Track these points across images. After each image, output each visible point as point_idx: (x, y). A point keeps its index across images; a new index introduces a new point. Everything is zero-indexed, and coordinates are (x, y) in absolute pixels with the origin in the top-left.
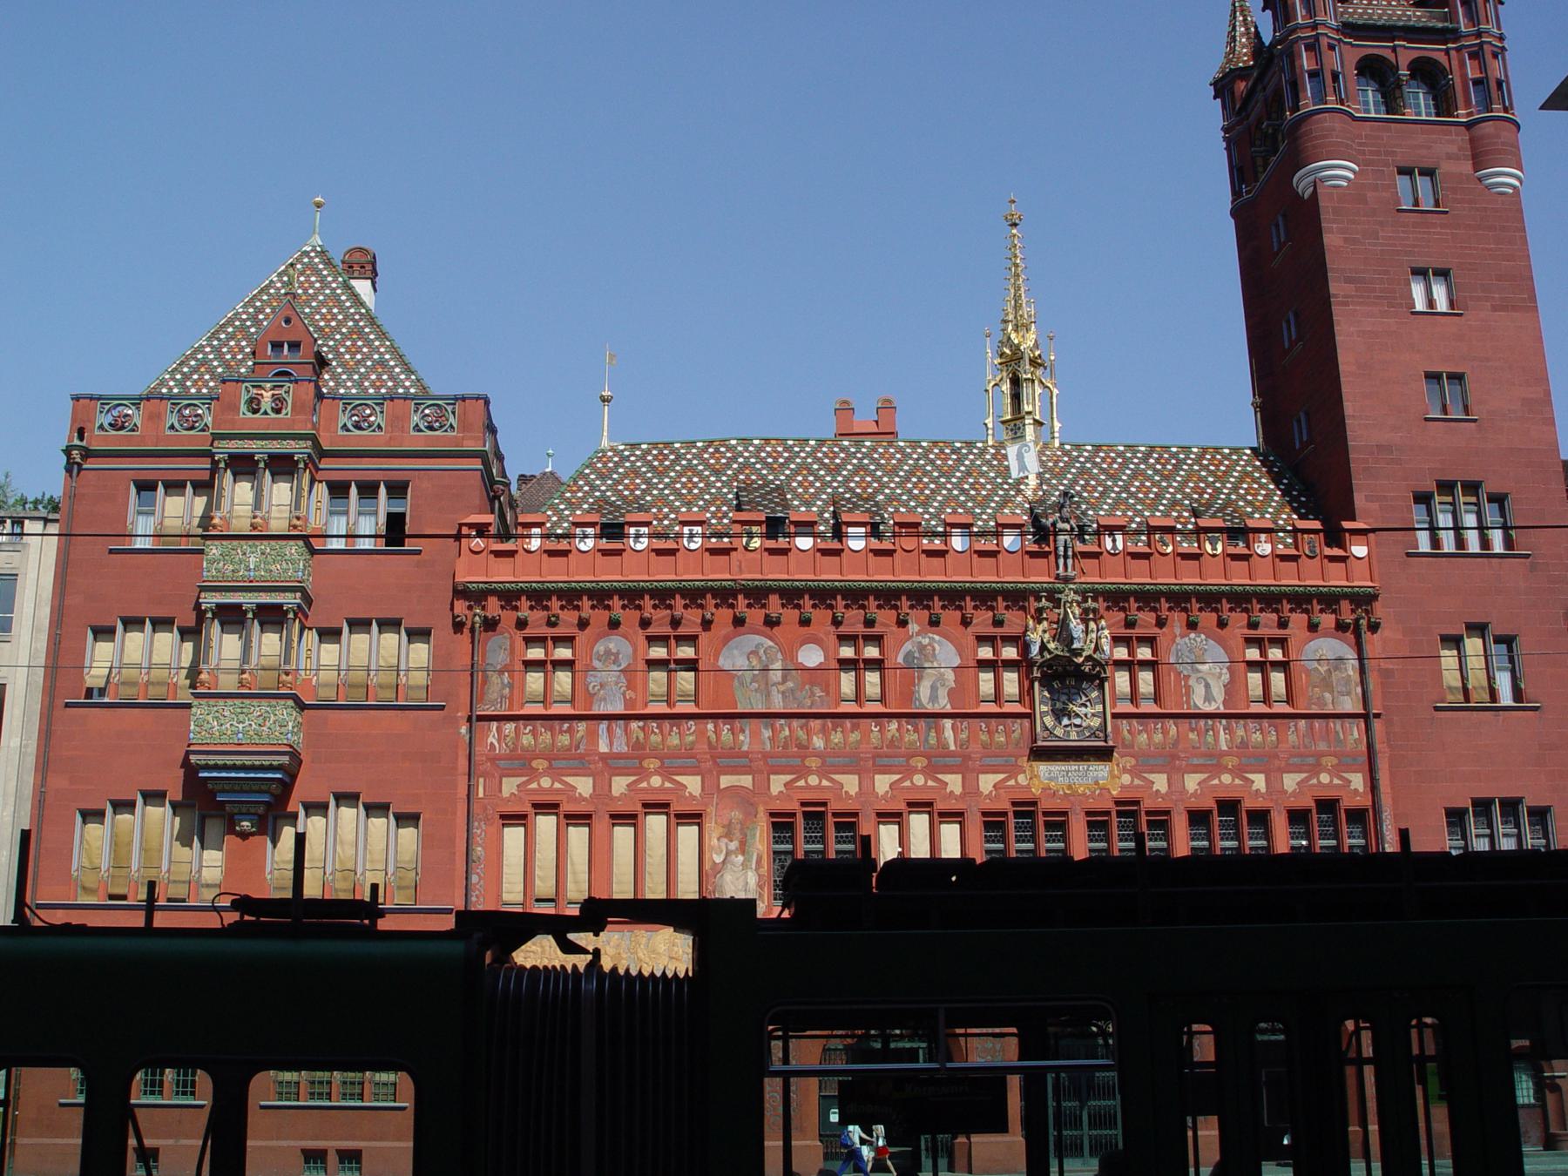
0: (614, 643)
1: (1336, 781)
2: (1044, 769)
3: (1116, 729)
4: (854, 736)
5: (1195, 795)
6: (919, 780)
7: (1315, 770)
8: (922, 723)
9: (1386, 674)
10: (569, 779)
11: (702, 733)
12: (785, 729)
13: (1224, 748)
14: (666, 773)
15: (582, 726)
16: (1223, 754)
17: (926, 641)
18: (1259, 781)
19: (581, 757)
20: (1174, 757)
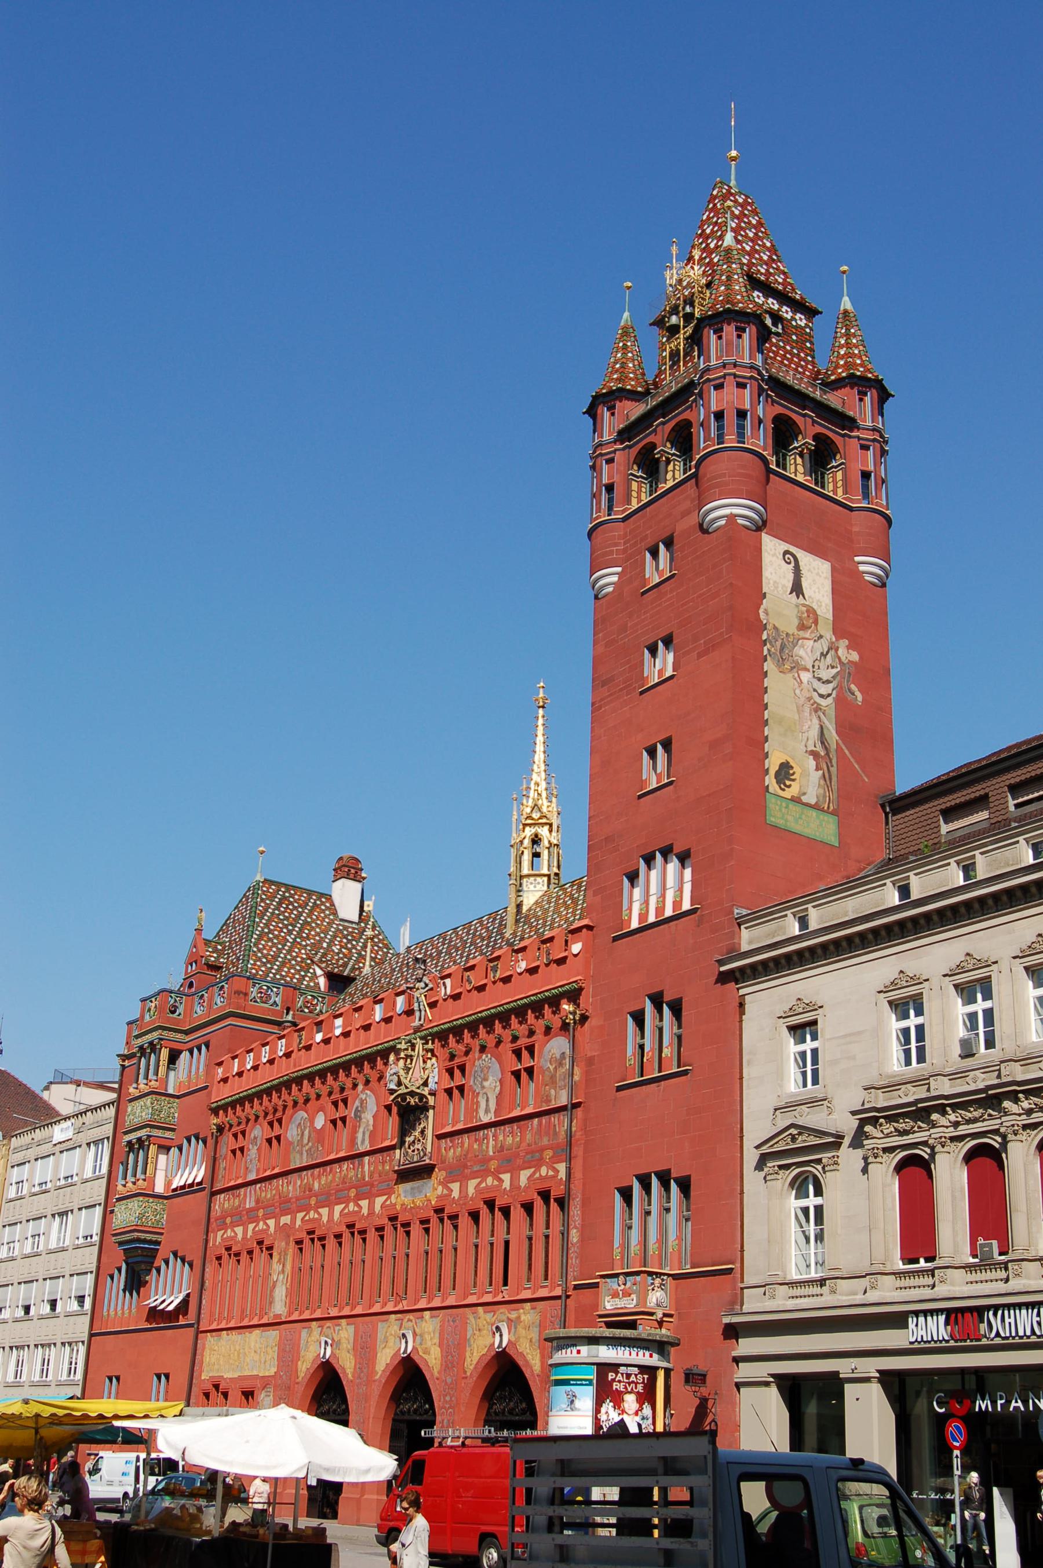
1: (551, 1173)
2: (403, 1188)
3: (439, 1148)
4: (330, 1178)
5: (472, 1199)
6: (352, 1207)
7: (538, 1164)
8: (356, 1161)
9: (590, 1061)
13: (491, 1153)
16: (492, 1158)
17: (364, 1096)
19: (239, 1214)
20: (465, 1166)
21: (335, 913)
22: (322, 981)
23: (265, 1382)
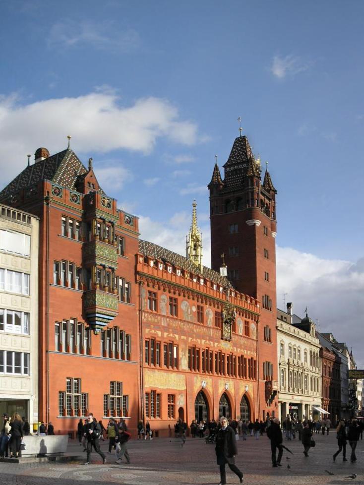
4: (200, 330)
10: (157, 331)
11: (178, 324)
12: (191, 326)
14: (173, 334)
15: (159, 318)
19: (159, 326)
23: (180, 392)
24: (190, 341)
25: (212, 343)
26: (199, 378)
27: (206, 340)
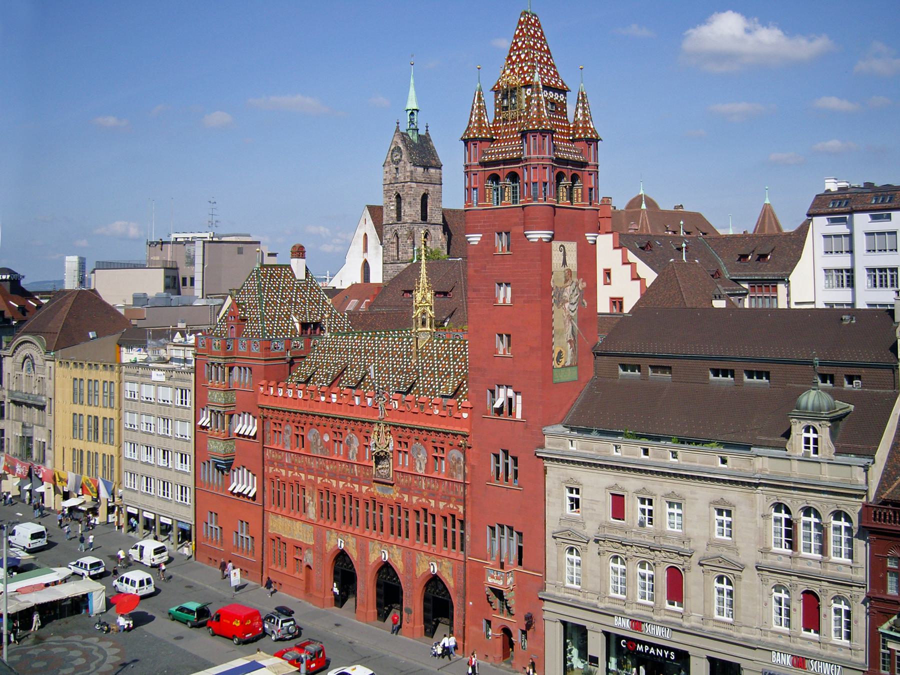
0: (288, 427)
7: (449, 502)
12: (322, 462)
18: (433, 502)
21: (294, 277)
22: (298, 326)
23: (308, 547)
24: (319, 482)
25: (356, 486)
26: (334, 535)
27: (347, 482)
